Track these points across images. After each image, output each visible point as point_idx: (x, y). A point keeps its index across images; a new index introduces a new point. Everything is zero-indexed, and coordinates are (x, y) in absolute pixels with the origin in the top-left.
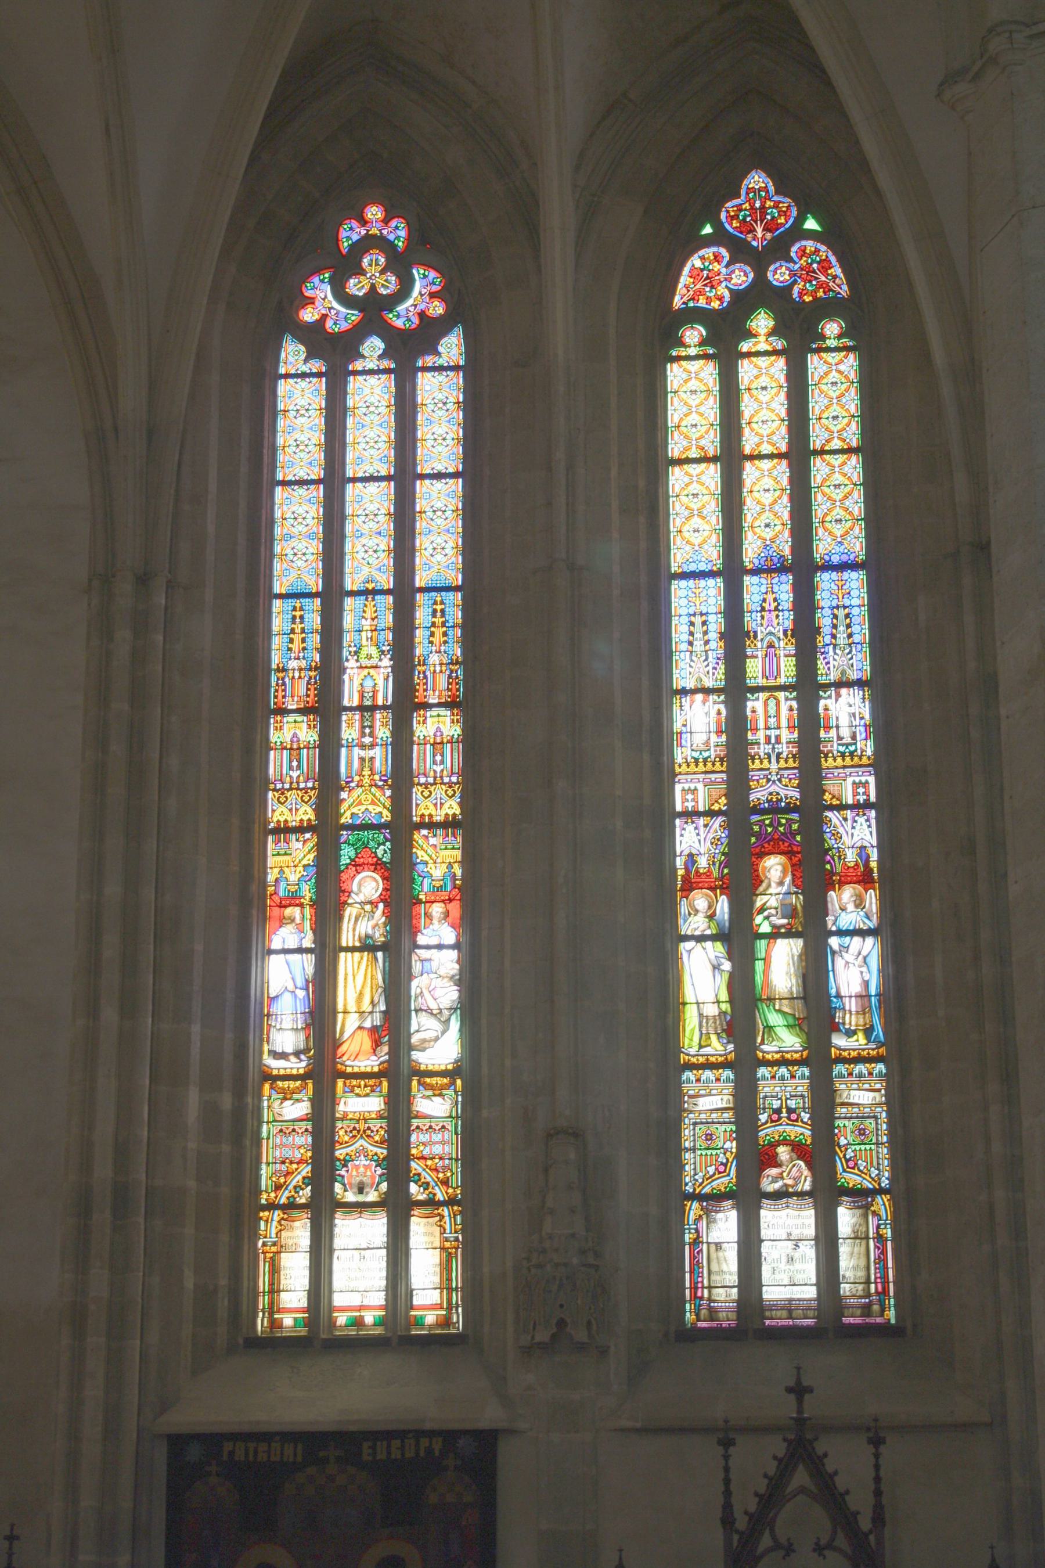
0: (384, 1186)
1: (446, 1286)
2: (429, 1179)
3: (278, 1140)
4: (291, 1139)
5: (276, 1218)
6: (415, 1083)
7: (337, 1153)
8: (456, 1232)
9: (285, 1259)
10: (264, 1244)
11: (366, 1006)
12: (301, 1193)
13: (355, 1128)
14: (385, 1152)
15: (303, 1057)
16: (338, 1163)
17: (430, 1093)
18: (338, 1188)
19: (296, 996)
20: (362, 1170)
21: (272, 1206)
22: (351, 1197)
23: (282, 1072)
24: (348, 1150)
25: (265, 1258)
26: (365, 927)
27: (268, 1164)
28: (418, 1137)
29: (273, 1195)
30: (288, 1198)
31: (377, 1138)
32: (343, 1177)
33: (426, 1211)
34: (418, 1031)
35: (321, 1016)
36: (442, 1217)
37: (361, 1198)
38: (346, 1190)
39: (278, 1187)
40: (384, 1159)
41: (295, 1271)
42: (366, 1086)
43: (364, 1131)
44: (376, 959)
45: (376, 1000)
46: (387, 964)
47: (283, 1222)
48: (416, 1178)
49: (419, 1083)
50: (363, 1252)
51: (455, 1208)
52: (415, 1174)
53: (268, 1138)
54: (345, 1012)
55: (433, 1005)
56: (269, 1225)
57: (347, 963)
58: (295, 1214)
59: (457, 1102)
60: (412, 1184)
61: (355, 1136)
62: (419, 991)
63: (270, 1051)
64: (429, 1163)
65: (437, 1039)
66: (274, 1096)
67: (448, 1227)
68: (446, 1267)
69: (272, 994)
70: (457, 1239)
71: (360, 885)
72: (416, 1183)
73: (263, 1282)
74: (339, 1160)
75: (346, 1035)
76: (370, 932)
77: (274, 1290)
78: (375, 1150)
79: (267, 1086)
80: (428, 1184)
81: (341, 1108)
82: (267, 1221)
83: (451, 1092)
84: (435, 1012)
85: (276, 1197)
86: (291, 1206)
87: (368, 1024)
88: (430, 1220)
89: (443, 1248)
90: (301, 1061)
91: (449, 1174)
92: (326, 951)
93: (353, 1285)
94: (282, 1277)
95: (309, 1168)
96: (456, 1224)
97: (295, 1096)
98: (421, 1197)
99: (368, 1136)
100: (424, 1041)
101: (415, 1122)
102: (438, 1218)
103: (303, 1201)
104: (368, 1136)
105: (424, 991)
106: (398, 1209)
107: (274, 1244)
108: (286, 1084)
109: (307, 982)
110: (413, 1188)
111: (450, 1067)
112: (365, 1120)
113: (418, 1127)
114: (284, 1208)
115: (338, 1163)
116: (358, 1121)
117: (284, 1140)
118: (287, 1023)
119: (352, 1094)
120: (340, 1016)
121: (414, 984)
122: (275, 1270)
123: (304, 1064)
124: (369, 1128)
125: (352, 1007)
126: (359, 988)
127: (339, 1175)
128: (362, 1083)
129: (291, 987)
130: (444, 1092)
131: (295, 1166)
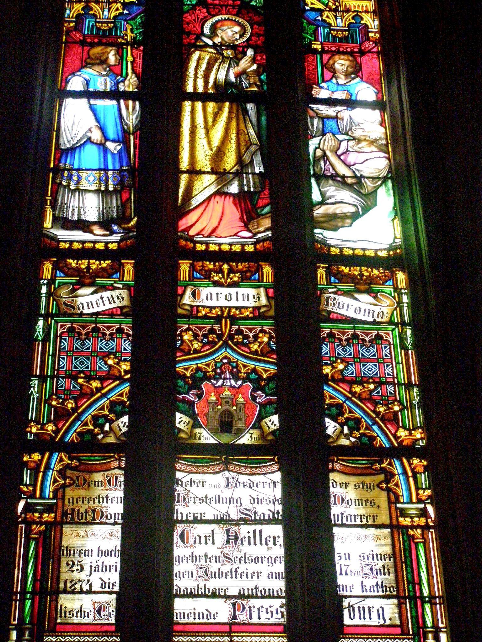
0: (273, 422)
1: (405, 593)
2: (359, 413)
3: (65, 344)
4: (89, 343)
5: (55, 465)
6: (321, 272)
7: (180, 367)
8: (419, 501)
9: (74, 537)
10: (28, 508)
11: (230, 161)
12: (107, 427)
13: (212, 331)
14: (273, 369)
15: (115, 228)
16: (181, 383)
17: (349, 287)
18: (181, 420)
19: (106, 150)
20: (227, 393)
21: (46, 445)
22: (206, 437)
23: (76, 246)
24: (201, 363)
25: (29, 531)
26: (221, 74)
27: (42, 378)
28: (333, 349)
29: (50, 428)
30: (80, 434)
31: (255, 347)
32: (191, 404)
33: (361, 463)
34: (322, 203)
35: (149, 172)
36: (389, 476)
37: (225, 439)
38: (196, 425)
39: (61, 415)
40: (270, 379)
41: (96, 554)
42: (231, 271)
43: (231, 337)
44: (245, 112)
45: (247, 158)
46: (263, 118)
47: (69, 473)
48: (334, 411)
49: (329, 273)
50: (233, 529)
51: (416, 461)
52: (330, 405)
53: (46, 339)
54: (194, 172)
55: (342, 170)
56: (45, 478)
57: (192, 115)
58: (93, 459)
59: (400, 303)
60: (327, 420)
61: (213, 343)
62: (319, 153)
63: (55, 219)
64: (357, 389)
65: (355, 216)
66: (61, 278)
67: (403, 492)
68: (402, 559)
69: (65, 143)
70: (424, 513)
71: (214, 28)
72: (335, 419)
73: (25, 573)
74: (184, 377)
75: (195, 202)
76: (232, 78)
77: (49, 588)
78: (252, 364)
79: (48, 266)
80: (358, 421)
81: (187, 299)
82: (35, 471)
83: (388, 288)
84: (349, 181)
85: (57, 432)
86: (88, 444)
87: (234, 188)
88: (368, 479)
89: (394, 527)
90: (112, 233)
91: (397, 408)
92: (160, 100)
93: (213, 584)
94: (64, 568)
95: (126, 388)
96: (417, 489)
97: (99, 281)
98: (344, 442)
99: (237, 344)
100: (334, 217)
101: (326, 328)
102: (382, 477)
103: (111, 439)
104: (237, 344)
105: (328, 153)
106: (305, 465)
107: (49, 509)
108: (83, 264)
109: (125, 133)
110: (331, 426)
111: (384, 254)
112: (233, 319)
113: (331, 335)
114: (70, 449)
115: (181, 383)
116: (218, 319)
117: (77, 344)
118: (89, 181)
119: (206, 282)
120: (184, 179)
121: (313, 143)
122: (51, 552)
123: (117, 237)
124: (239, 332)
125: (204, 161)
126: (216, 143)
127: (183, 401)
128: (225, 267)
129: (97, 136)
130: (376, 287)
131: (95, 384)
